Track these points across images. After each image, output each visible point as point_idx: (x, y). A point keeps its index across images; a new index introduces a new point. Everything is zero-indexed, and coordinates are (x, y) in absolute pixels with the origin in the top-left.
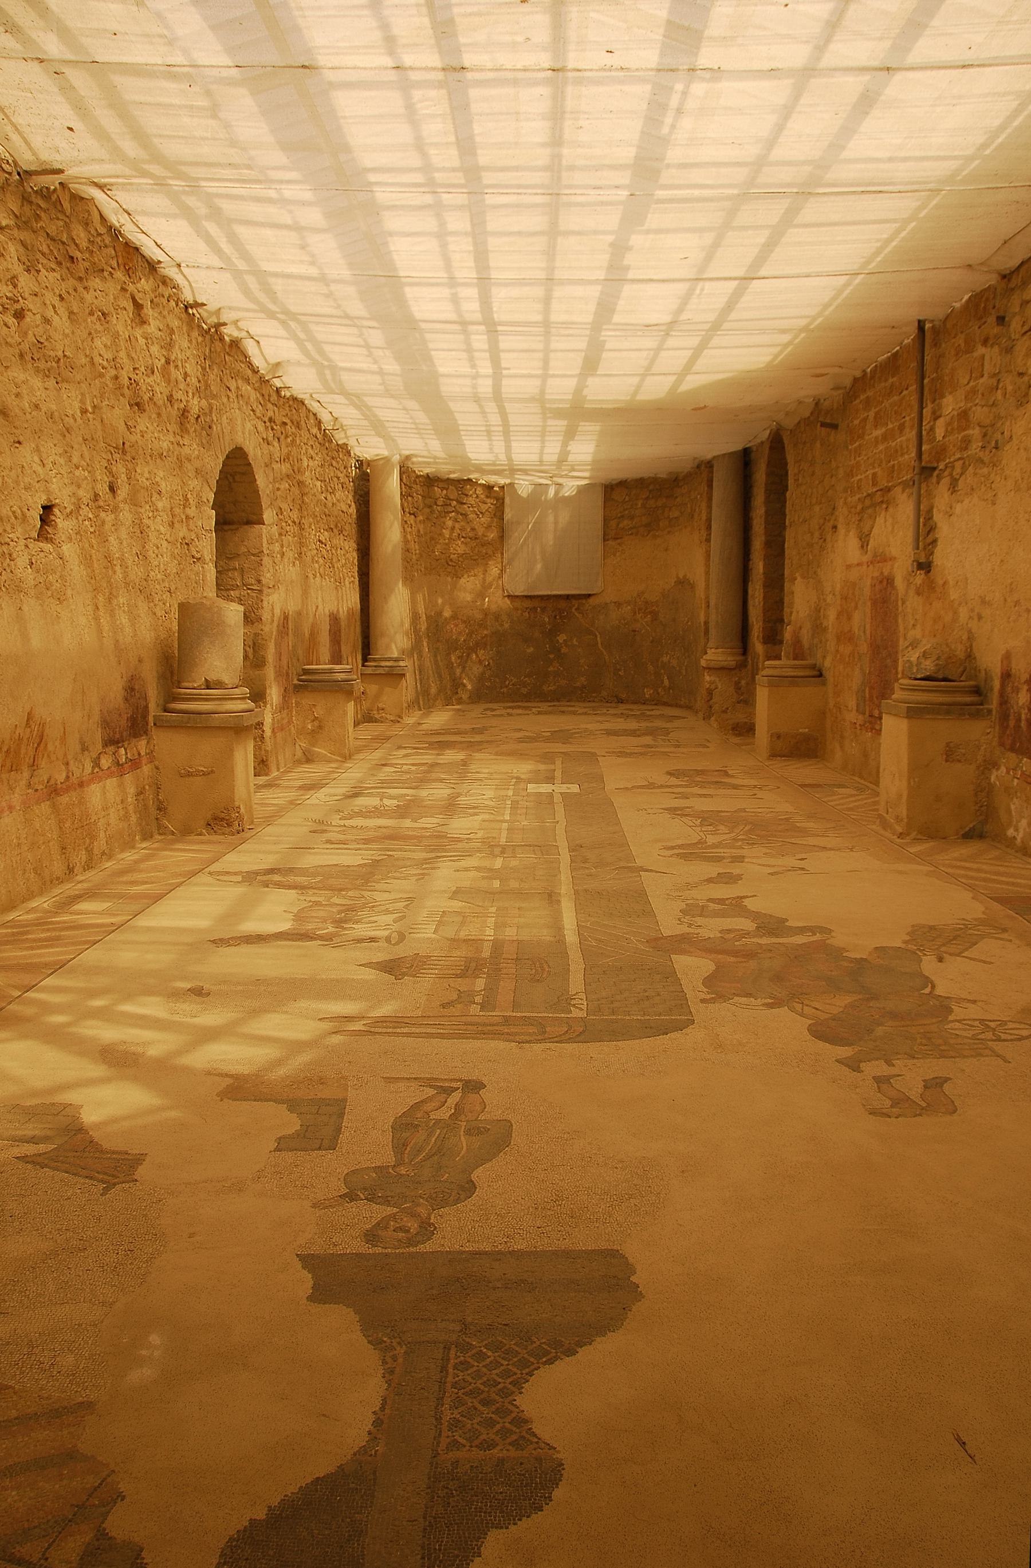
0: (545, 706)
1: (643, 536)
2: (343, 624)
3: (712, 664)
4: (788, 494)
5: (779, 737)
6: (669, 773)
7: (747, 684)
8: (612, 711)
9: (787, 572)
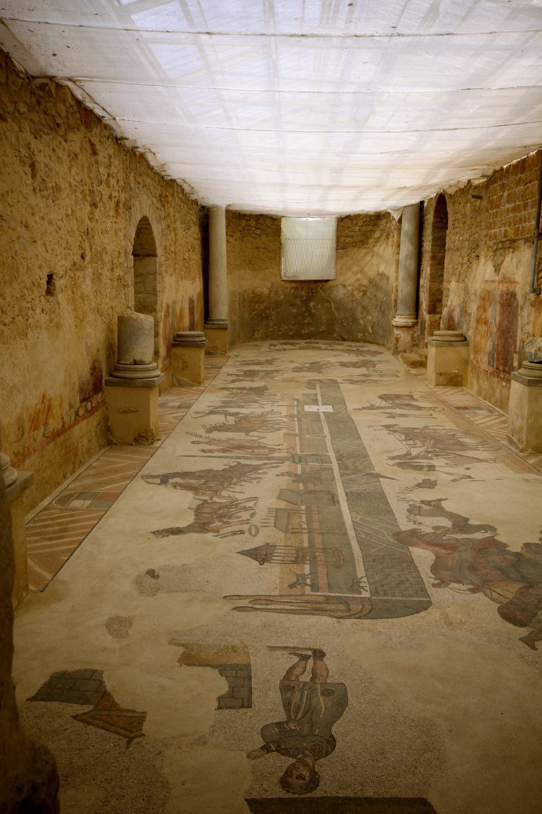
0: (302, 343)
1: (359, 247)
2: (195, 302)
3: (399, 324)
4: (448, 231)
5: (441, 375)
6: (381, 397)
7: (418, 336)
8: (340, 347)
9: (445, 277)
